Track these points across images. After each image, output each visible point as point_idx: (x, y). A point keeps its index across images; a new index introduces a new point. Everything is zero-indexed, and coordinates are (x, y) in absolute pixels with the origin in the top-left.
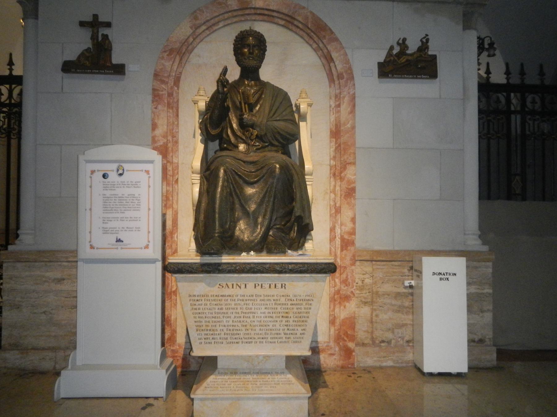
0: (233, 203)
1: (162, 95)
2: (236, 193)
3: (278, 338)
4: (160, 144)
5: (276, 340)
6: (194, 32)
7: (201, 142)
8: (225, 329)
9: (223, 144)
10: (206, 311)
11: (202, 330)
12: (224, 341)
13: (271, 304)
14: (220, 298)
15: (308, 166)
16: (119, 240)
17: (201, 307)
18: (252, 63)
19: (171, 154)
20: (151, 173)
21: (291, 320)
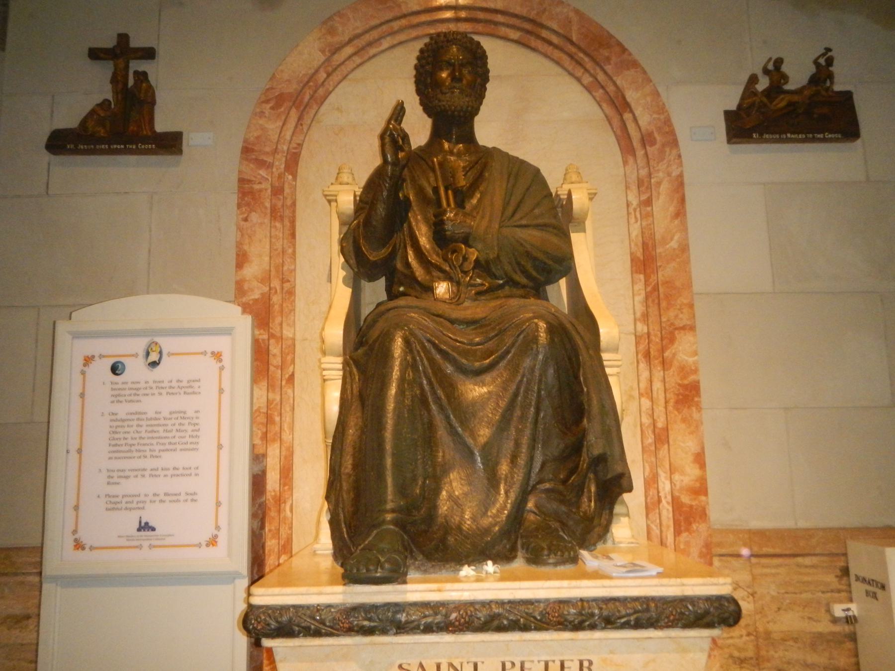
0: (431, 427)
1: (260, 191)
2: (437, 399)
4: (253, 297)
6: (328, 60)
7: (345, 282)
9: (395, 287)
15: (607, 331)
16: (144, 527)
18: (456, 100)
19: (278, 320)
20: (226, 358)
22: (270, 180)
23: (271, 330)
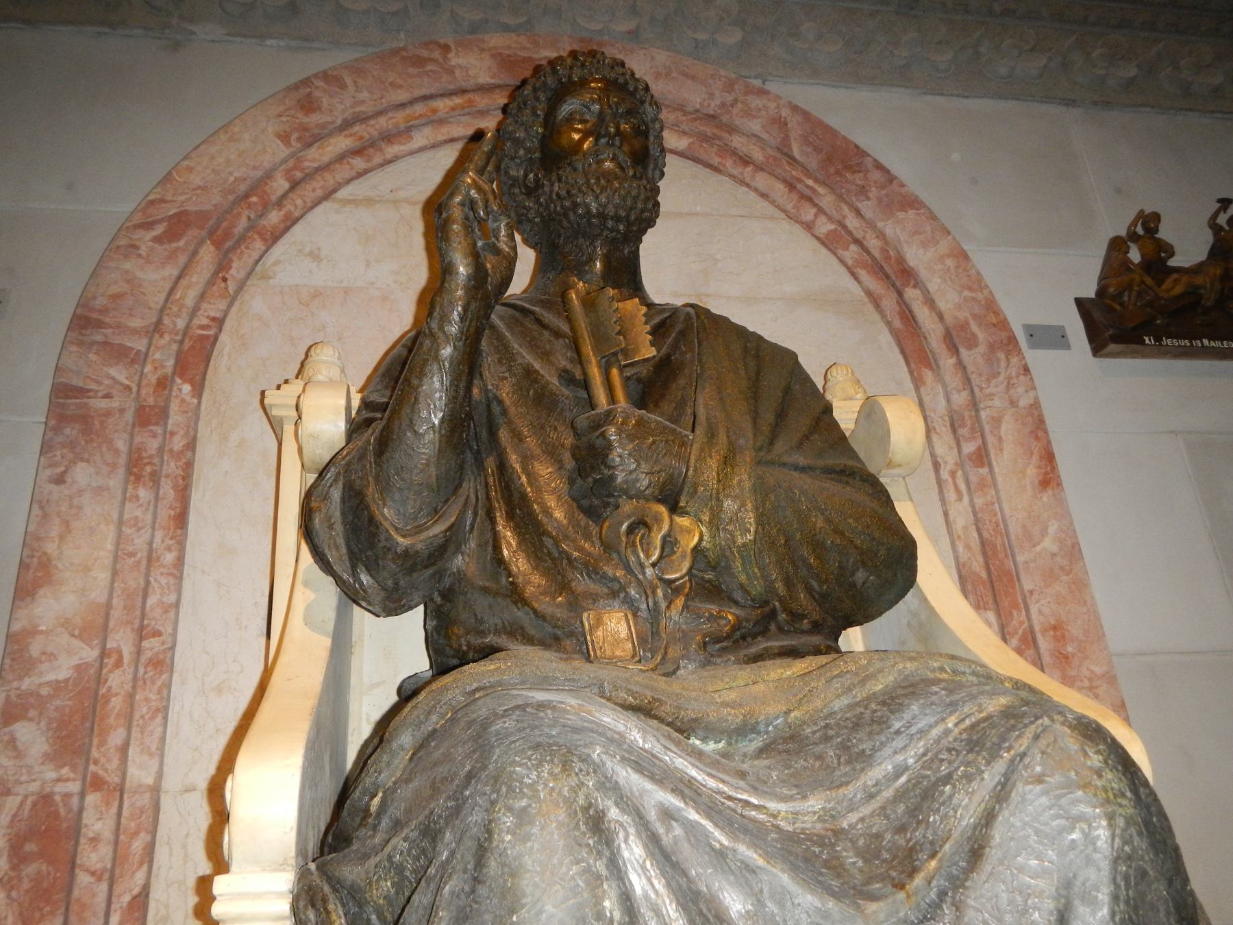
1: (108, 413)
4: (51, 677)
22: (135, 389)
23: (92, 768)
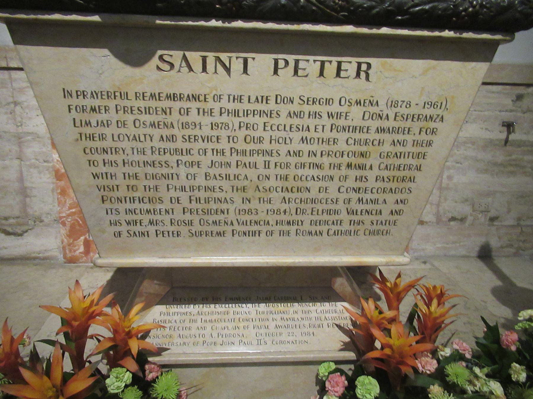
3: (330, 223)
5: (325, 228)
8: (184, 197)
10: (126, 144)
11: (119, 200)
12: (184, 230)
13: (320, 128)
14: (166, 104)
17: (107, 131)
21: (371, 175)
